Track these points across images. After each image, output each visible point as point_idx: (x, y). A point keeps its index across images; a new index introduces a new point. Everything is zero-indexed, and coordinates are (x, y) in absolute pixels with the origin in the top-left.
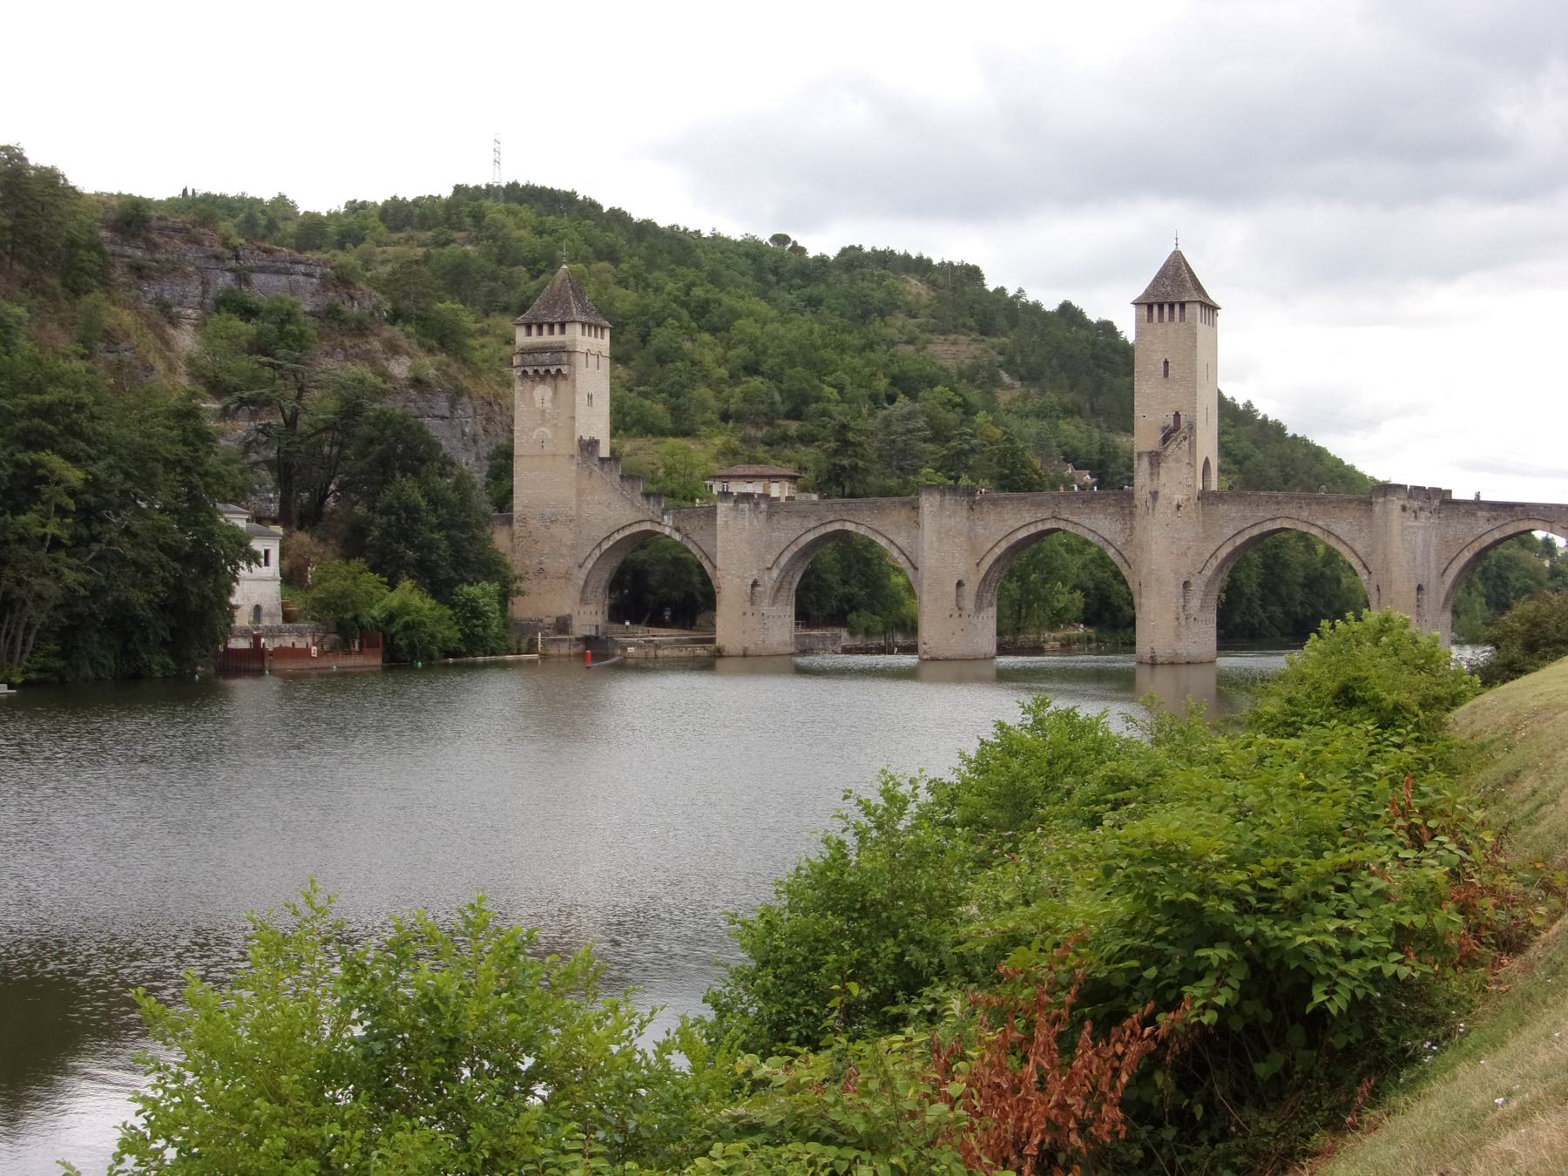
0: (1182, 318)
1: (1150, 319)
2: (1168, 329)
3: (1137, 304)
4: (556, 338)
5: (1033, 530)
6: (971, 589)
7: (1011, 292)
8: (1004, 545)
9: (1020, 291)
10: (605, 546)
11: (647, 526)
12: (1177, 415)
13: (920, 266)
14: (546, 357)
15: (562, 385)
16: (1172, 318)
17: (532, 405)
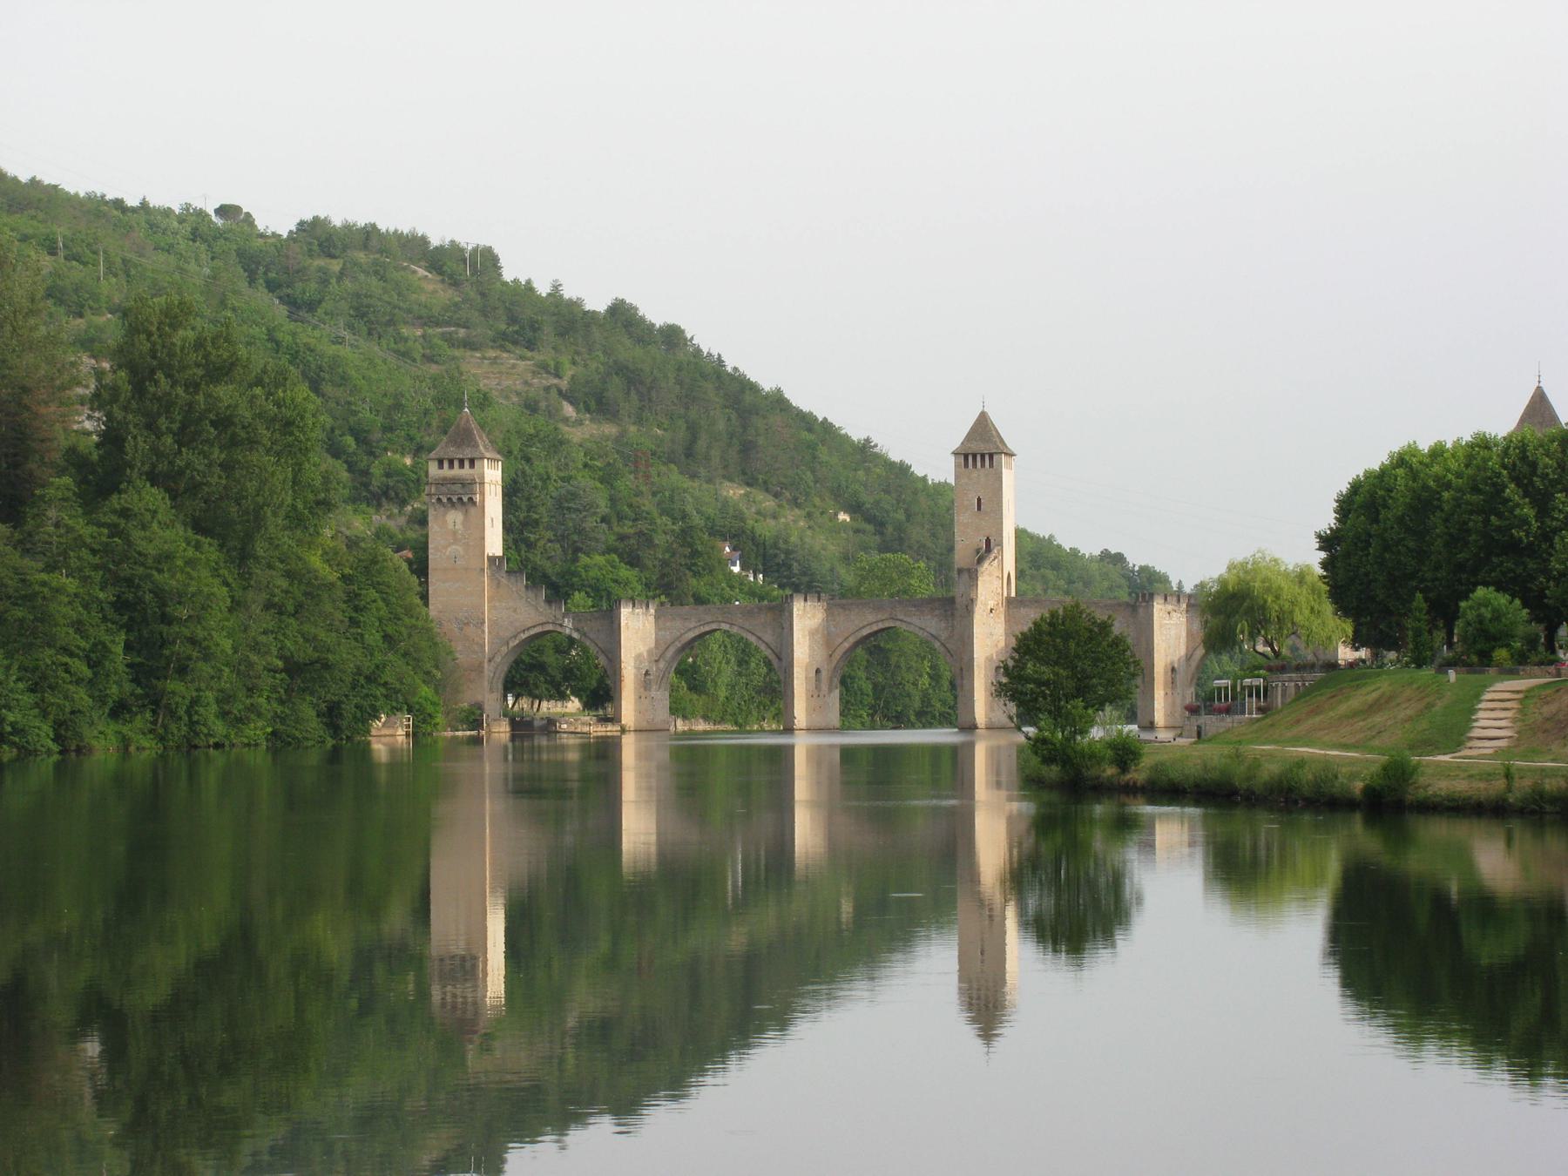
0: (991, 465)
1: (966, 465)
2: (979, 474)
3: (955, 453)
4: (466, 471)
5: (875, 628)
6: (824, 674)
7: (543, 289)
8: (852, 640)
9: (556, 287)
10: (512, 644)
11: (550, 627)
12: (988, 541)
13: (414, 246)
14: (457, 488)
15: (473, 511)
16: (983, 465)
17: (444, 526)
